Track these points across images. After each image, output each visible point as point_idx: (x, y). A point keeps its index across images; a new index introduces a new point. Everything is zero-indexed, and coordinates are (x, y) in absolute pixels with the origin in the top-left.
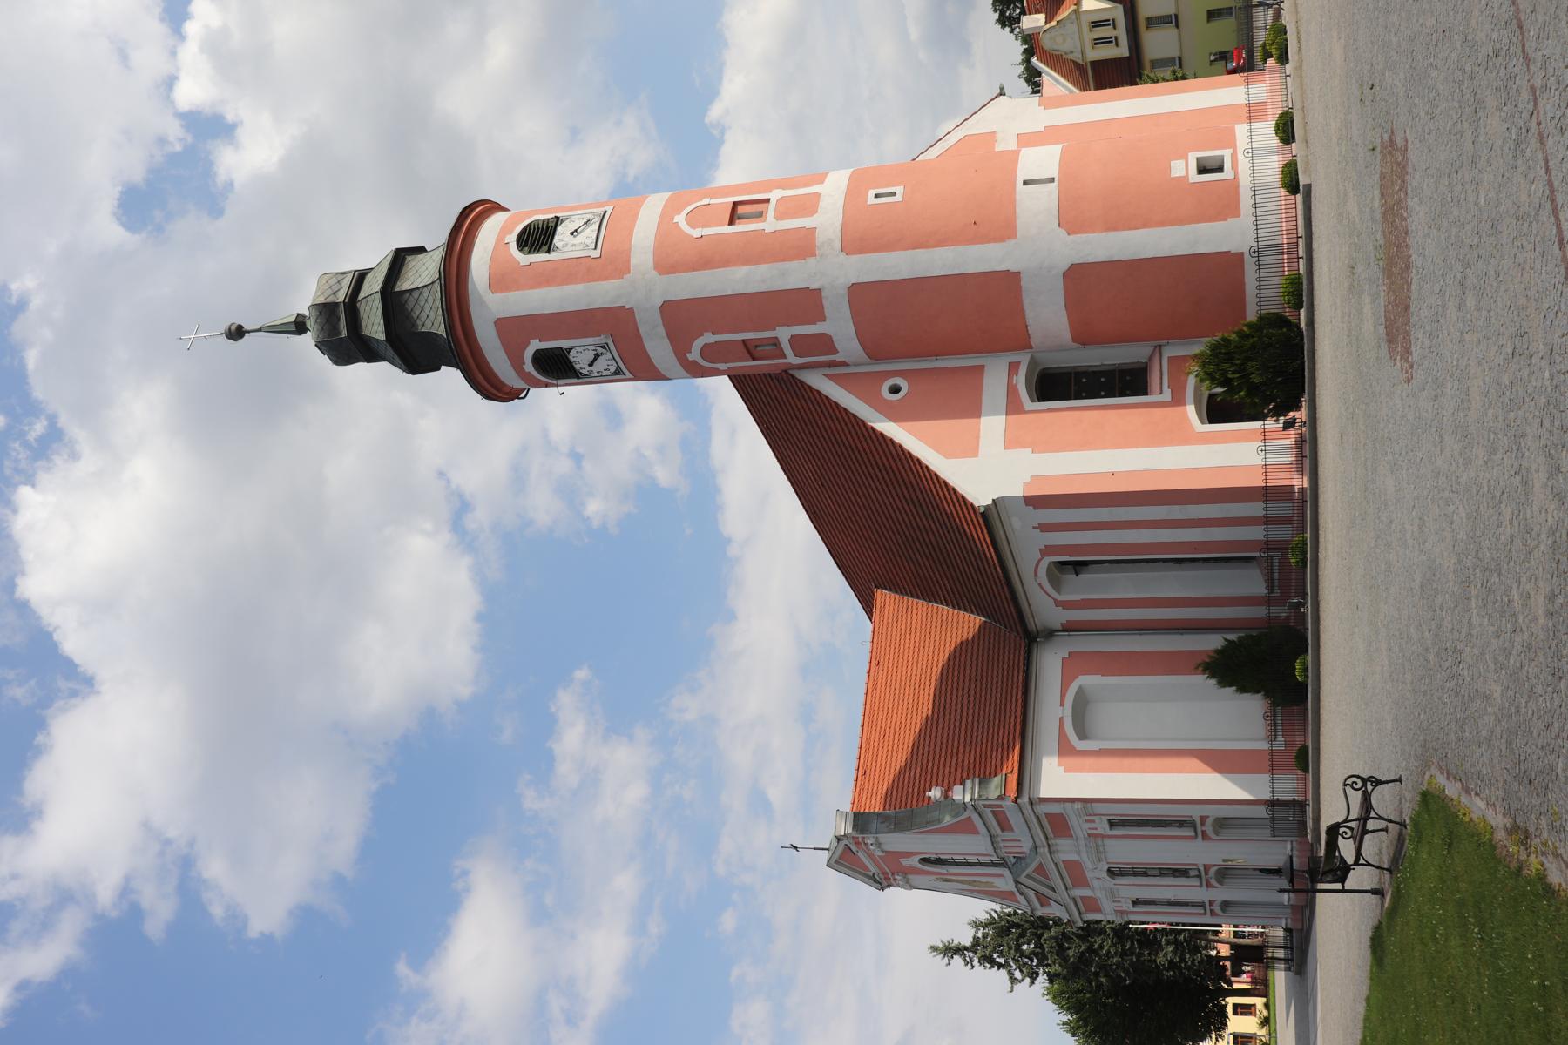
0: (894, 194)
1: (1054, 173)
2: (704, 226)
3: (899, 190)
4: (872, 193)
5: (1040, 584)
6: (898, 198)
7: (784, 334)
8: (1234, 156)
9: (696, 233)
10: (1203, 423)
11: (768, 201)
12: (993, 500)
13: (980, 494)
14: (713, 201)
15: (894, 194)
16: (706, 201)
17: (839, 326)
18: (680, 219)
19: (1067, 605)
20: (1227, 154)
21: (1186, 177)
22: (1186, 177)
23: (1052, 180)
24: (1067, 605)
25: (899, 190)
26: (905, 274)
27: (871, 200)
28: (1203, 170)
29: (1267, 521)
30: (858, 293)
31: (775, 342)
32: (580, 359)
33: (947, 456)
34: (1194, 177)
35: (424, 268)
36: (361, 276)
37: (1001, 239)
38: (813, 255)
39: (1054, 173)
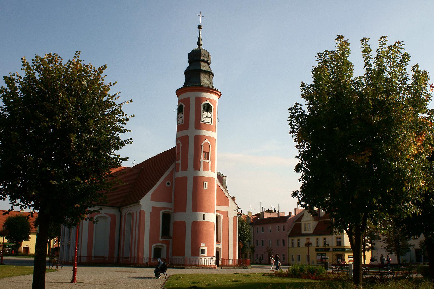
0: (206, 187)
1: (205, 220)
2: (204, 146)
4: (207, 182)
5: (128, 211)
6: (205, 188)
7: (180, 162)
8: (205, 256)
9: (203, 144)
10: (154, 246)
11: (208, 159)
12: (141, 204)
13: (142, 201)
15: (206, 187)
16: (210, 146)
17: (180, 174)
18: (207, 141)
19: (125, 215)
20: (206, 255)
24: (125, 215)
25: (207, 188)
27: (205, 182)
29: (134, 258)
31: (179, 160)
32: (181, 115)
33: (152, 195)
39: (206, 220)
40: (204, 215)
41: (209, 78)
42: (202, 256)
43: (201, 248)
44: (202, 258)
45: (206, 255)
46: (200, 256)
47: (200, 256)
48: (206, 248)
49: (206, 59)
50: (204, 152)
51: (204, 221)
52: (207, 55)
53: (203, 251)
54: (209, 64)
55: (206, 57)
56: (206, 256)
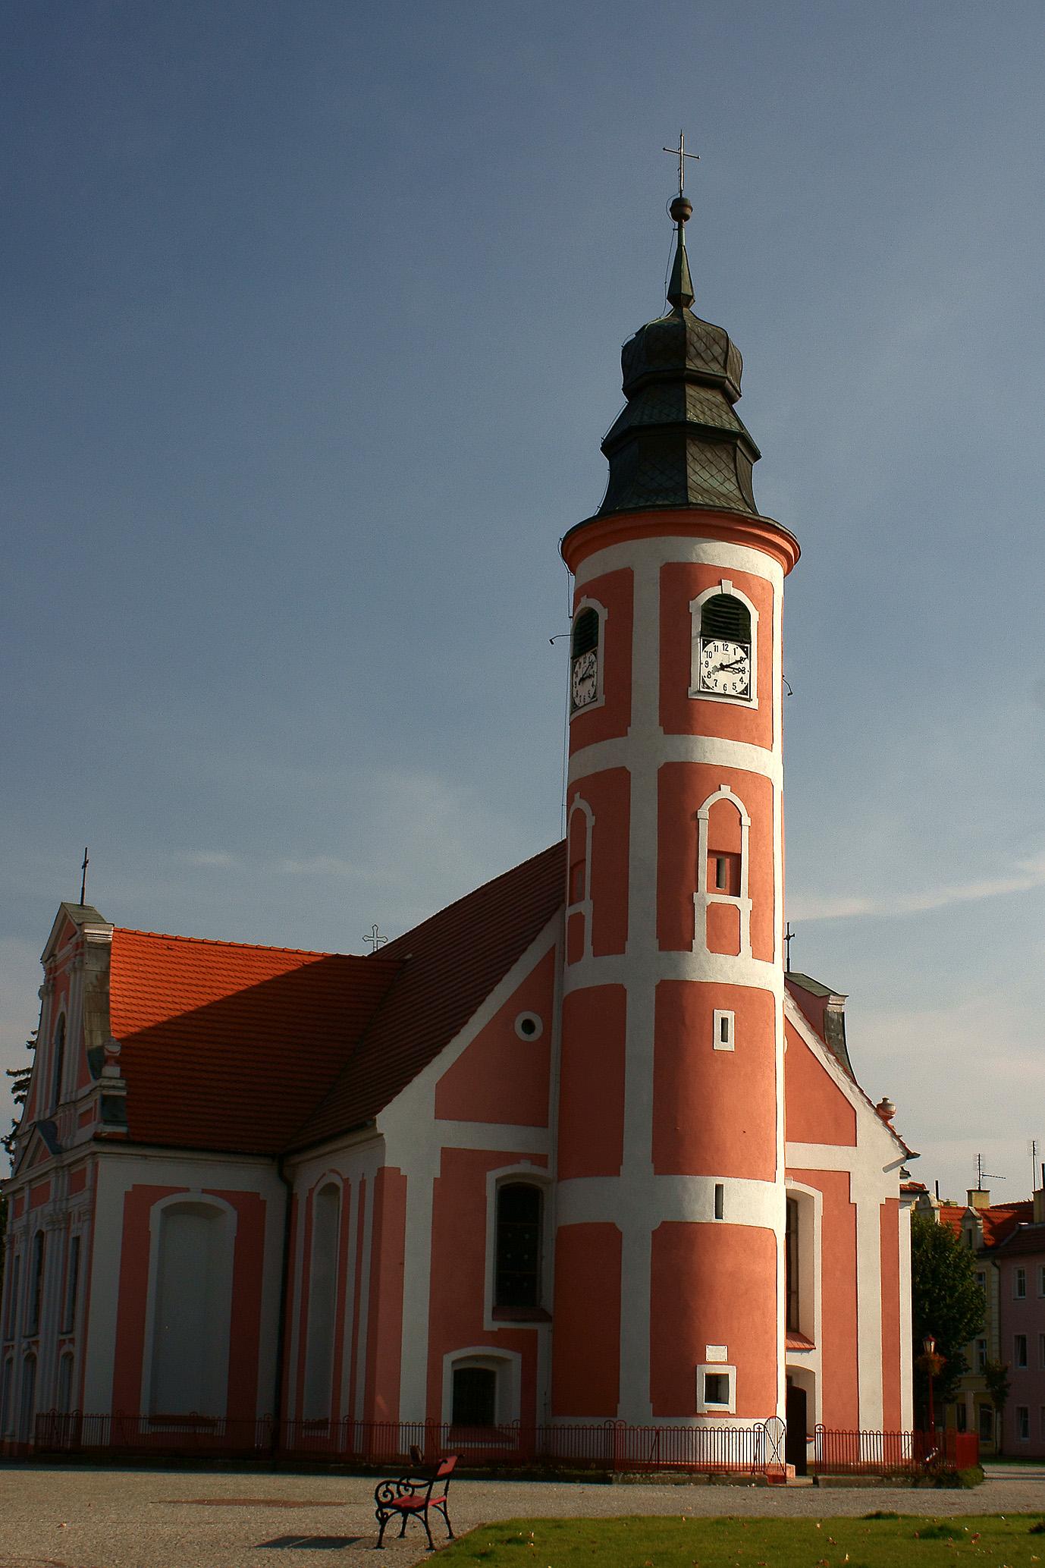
1: (730, 1217)
6: (719, 1045)
8: (727, 1415)
9: (704, 813)
14: (745, 830)
15: (724, 1039)
18: (726, 792)
20: (731, 1407)
21: (704, 1362)
23: (719, 1215)
25: (730, 1046)
26: (630, 1050)
30: (614, 997)
35: (714, 472)
37: (655, 1159)
38: (661, 948)
39: (730, 1217)
40: (719, 1188)
41: (732, 466)
42: (712, 1414)
43: (703, 1371)
44: (710, 1423)
45: (731, 1407)
46: (702, 1415)
47: (702, 1415)
48: (731, 1372)
49: (715, 369)
50: (711, 853)
51: (719, 1221)
52: (717, 350)
53: (716, 1388)
54: (731, 398)
55: (715, 359)
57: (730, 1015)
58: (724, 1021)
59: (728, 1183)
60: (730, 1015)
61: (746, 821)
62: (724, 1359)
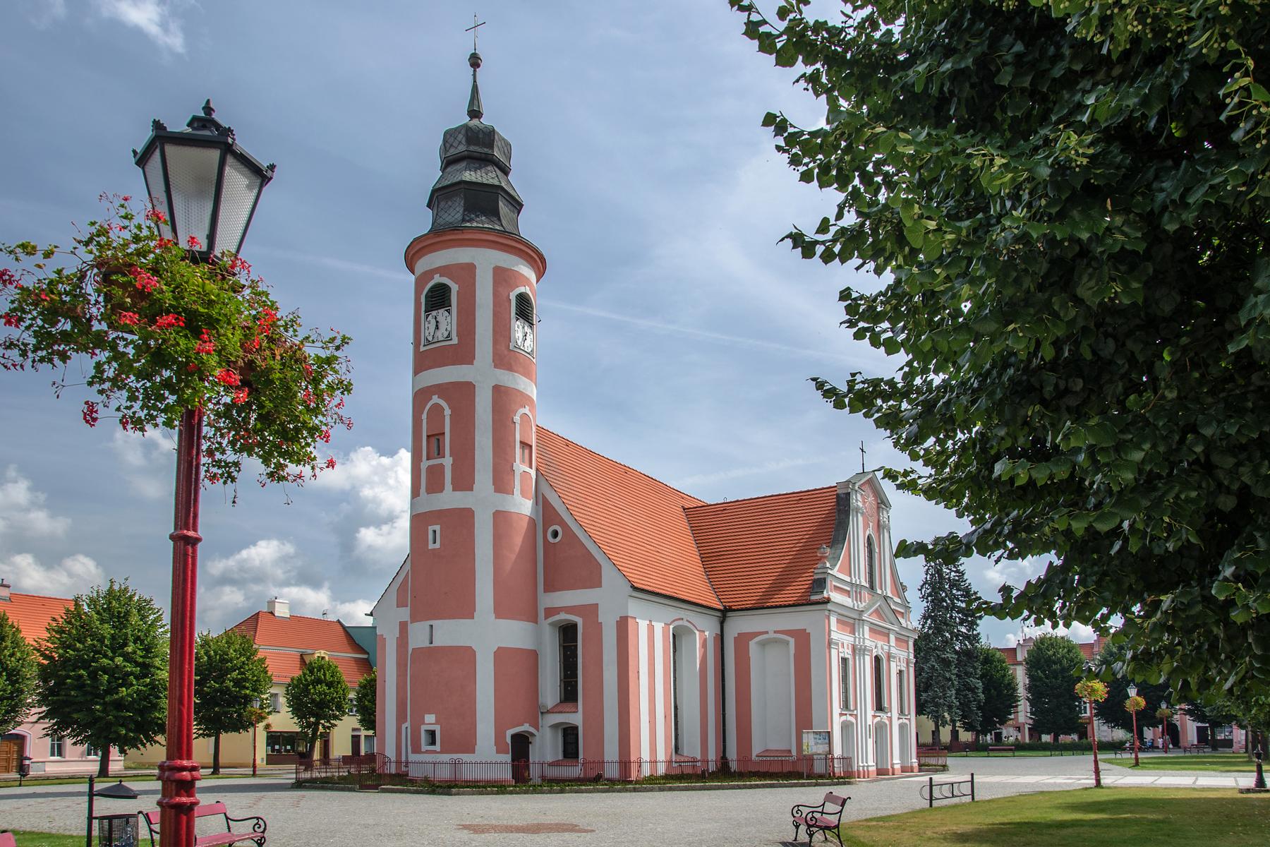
3: (438, 545)
8: (435, 752)
15: (435, 542)
20: (437, 747)
21: (424, 723)
22: (424, 723)
25: (438, 545)
27: (431, 529)
28: (432, 734)
34: (424, 728)
36: (505, 171)
40: (431, 626)
42: (427, 752)
43: (424, 728)
45: (437, 747)
48: (437, 728)
51: (431, 645)
56: (438, 753)
57: (437, 528)
58: (435, 532)
59: (435, 623)
60: (437, 528)
61: (448, 412)
62: (434, 722)
